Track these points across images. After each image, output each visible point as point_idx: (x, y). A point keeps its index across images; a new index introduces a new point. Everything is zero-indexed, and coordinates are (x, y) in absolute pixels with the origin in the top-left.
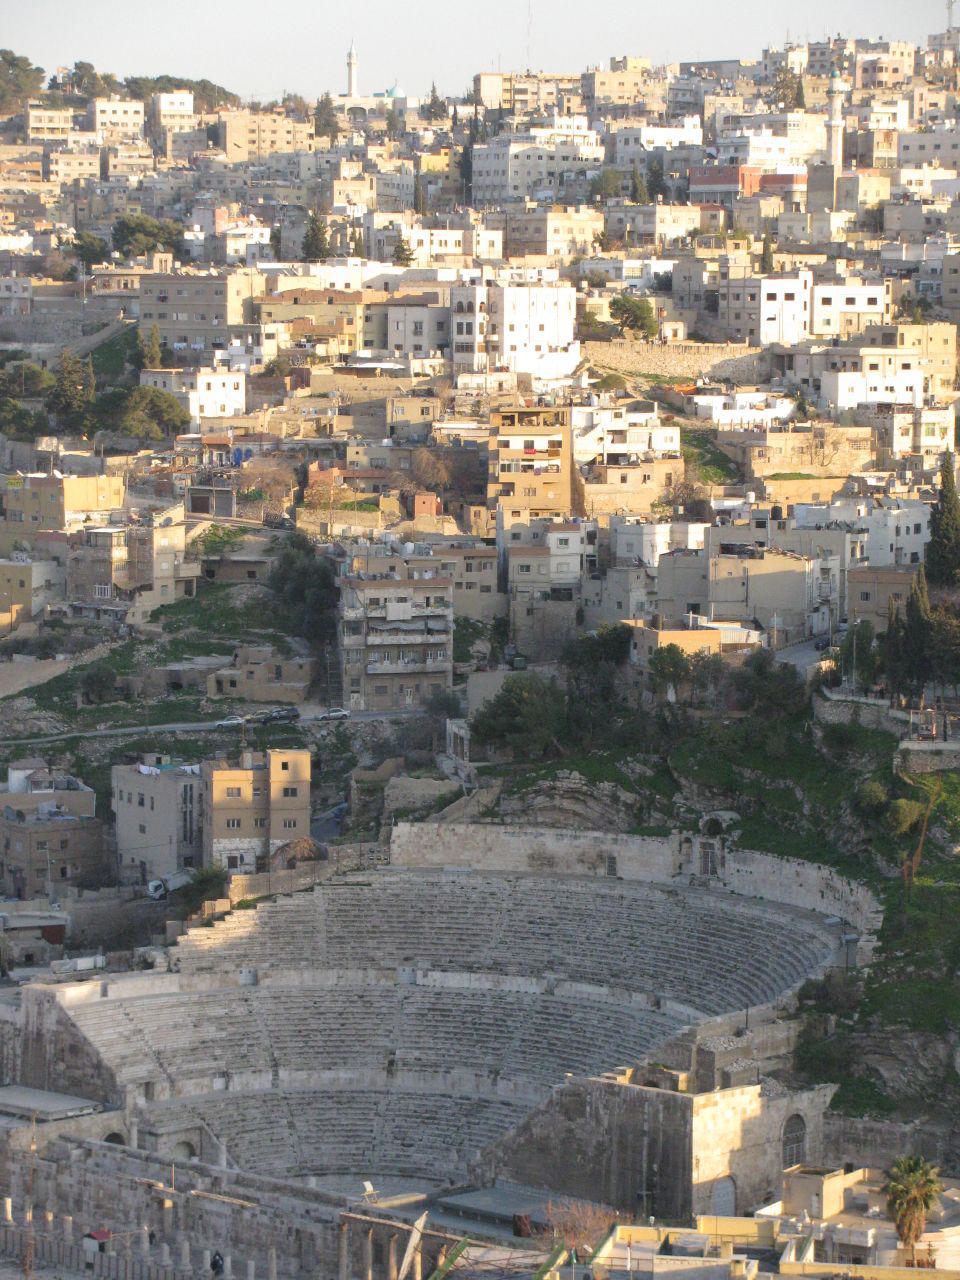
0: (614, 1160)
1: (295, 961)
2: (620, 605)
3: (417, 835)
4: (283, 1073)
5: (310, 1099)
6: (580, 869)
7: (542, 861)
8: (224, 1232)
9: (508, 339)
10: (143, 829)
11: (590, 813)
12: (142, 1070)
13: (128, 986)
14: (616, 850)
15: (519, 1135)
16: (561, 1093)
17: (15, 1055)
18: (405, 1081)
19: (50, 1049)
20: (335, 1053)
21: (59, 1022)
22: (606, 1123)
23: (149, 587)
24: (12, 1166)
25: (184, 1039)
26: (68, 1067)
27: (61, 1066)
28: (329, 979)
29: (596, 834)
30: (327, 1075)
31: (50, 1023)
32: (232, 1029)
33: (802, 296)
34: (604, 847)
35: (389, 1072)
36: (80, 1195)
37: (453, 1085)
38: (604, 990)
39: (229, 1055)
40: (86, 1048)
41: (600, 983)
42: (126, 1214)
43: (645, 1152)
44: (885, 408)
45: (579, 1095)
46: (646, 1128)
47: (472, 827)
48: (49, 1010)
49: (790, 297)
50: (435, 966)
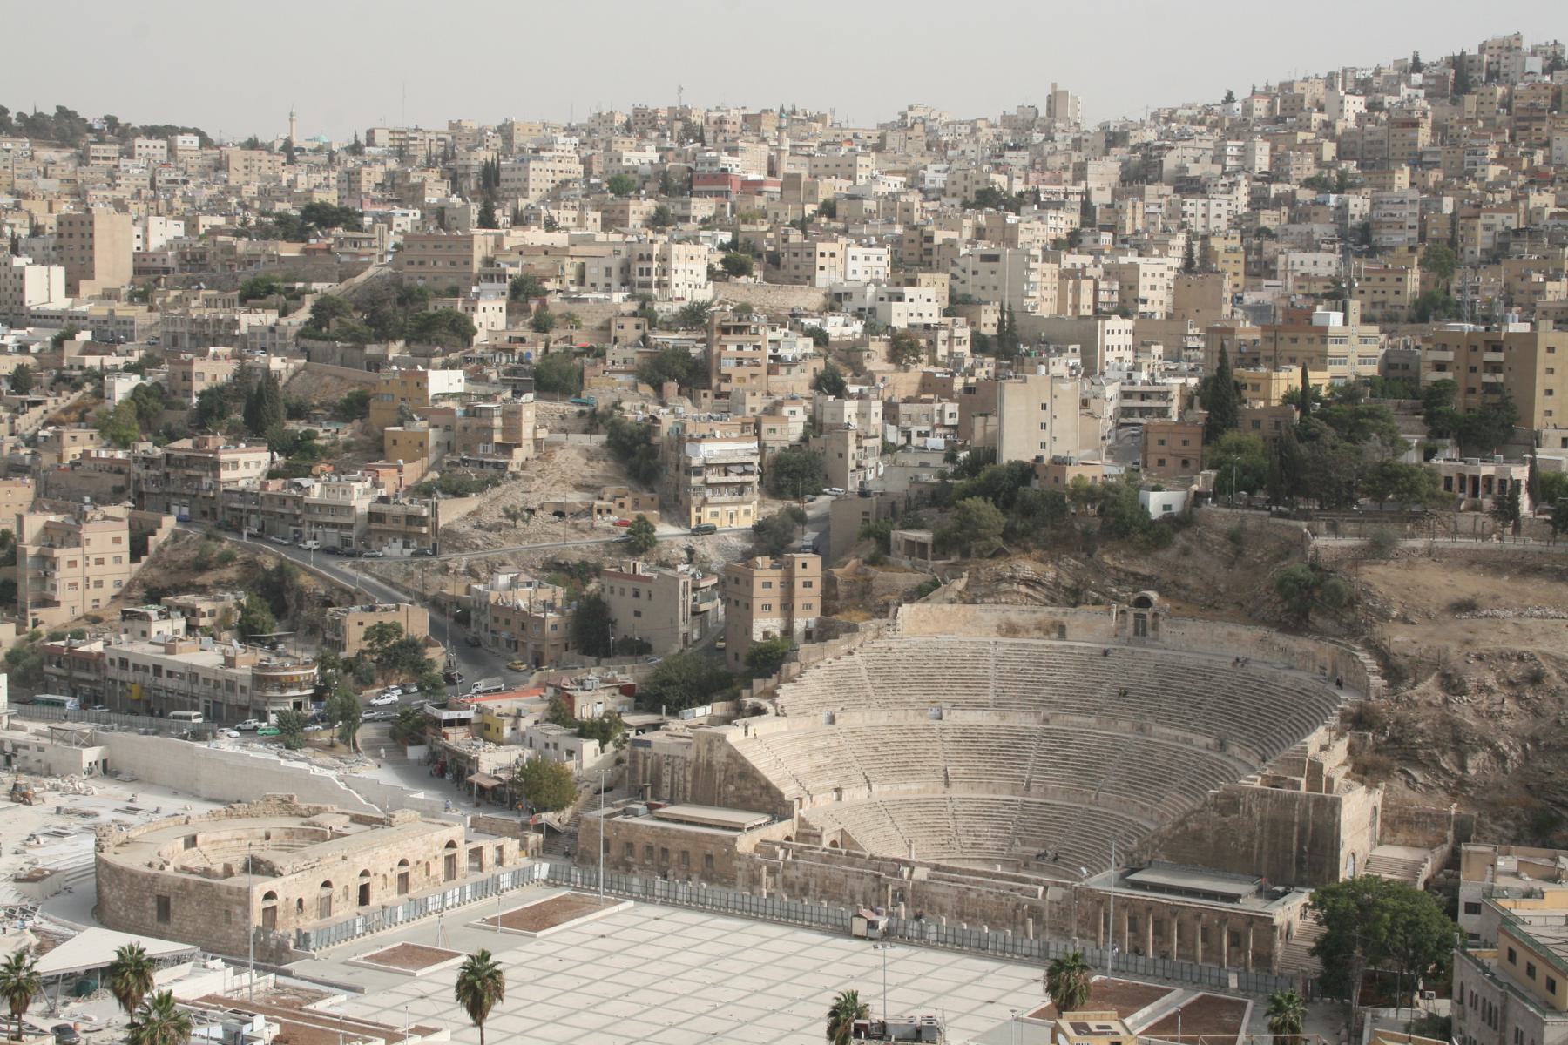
0: (1266, 847)
2: (841, 455)
4: (874, 787)
6: (1037, 633)
7: (1012, 630)
8: (950, 907)
9: (675, 279)
10: (638, 614)
11: (1037, 596)
13: (758, 725)
14: (1065, 620)
15: (1175, 828)
16: (1216, 796)
18: (958, 791)
19: (720, 777)
20: (903, 768)
23: (519, 446)
24: (737, 864)
25: (805, 766)
26: (738, 789)
27: (732, 788)
28: (882, 718)
30: (903, 787)
31: (720, 757)
33: (840, 254)
35: (947, 784)
36: (807, 884)
38: (1092, 720)
41: (1090, 715)
42: (852, 897)
47: (955, 607)
49: (833, 255)
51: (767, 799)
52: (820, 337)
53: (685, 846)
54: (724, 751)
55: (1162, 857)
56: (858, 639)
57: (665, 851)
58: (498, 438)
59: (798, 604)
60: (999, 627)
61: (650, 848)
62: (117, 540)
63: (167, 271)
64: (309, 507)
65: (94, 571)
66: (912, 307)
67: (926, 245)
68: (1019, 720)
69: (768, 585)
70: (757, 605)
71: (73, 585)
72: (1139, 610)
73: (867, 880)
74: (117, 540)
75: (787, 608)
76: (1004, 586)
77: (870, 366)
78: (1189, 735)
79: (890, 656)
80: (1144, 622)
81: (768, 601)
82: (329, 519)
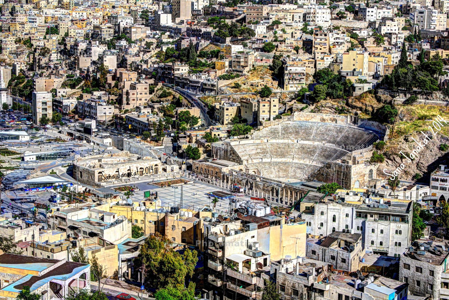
1: (275, 138)
5: (277, 164)
7: (323, 120)
9: (317, 19)
12: (246, 158)
18: (296, 161)
19: (229, 154)
25: (254, 152)
28: (281, 141)
31: (229, 149)
39: (262, 155)
44: (390, 34)
49: (372, 12)
52: (354, 36)
53: (213, 170)
55: (315, 179)
56: (281, 120)
58: (242, 64)
59: (272, 111)
62: (146, 89)
63: (201, 15)
64: (191, 82)
65: (139, 96)
66: (389, 28)
67: (408, 8)
68: (316, 143)
71: (134, 100)
74: (146, 89)
76: (323, 108)
77: (366, 45)
82: (195, 85)
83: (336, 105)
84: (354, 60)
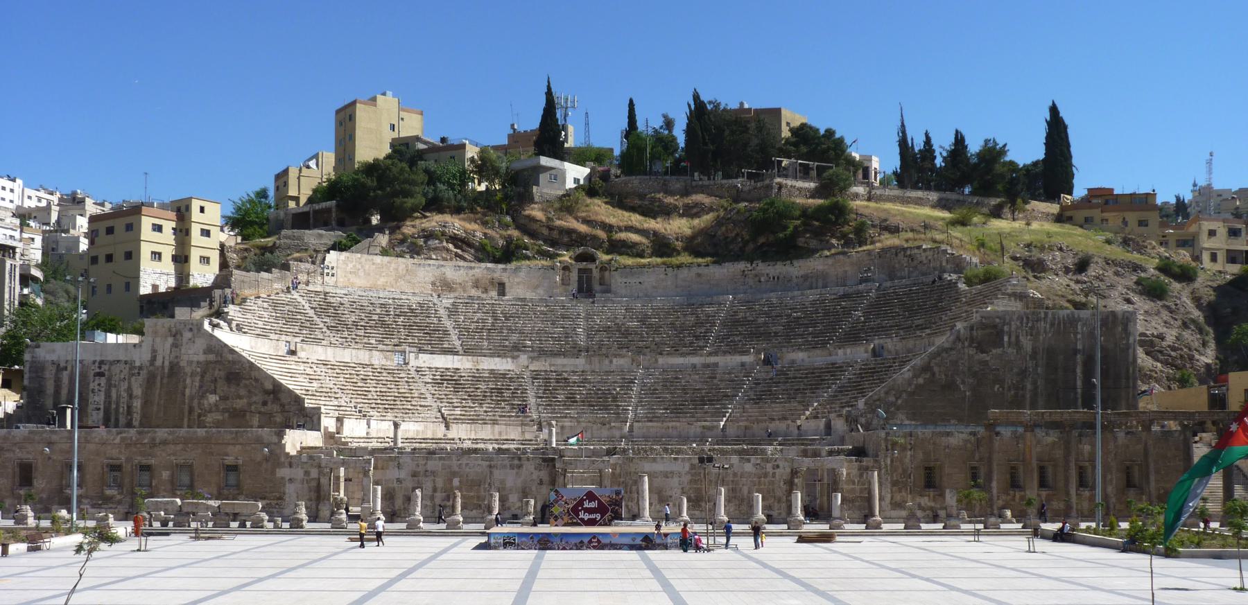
1: (317, 341)
3: (344, 262)
4: (373, 423)
7: (445, 286)
15: (916, 376)
17: (131, 396)
19: (191, 386)
21: (209, 350)
22: (1029, 349)
24: (284, 472)
26: (224, 398)
27: (213, 398)
29: (490, 265)
32: (315, 384)
34: (496, 275)
35: (447, 427)
37: (500, 433)
40: (253, 374)
43: (1079, 370)
45: (995, 326)
46: (1079, 347)
47: (386, 259)
48: (192, 341)
50: (421, 350)
51: (276, 408)
54: (200, 344)
57: (146, 468)
59: (195, 255)
60: (433, 284)
61: (115, 468)
69: (158, 228)
70: (145, 250)
72: (583, 265)
73: (529, 467)
75: (181, 259)
76: (434, 243)
78: (713, 359)
79: (332, 300)
80: (589, 279)
81: (157, 248)
83: (477, 231)
84: (393, 127)
